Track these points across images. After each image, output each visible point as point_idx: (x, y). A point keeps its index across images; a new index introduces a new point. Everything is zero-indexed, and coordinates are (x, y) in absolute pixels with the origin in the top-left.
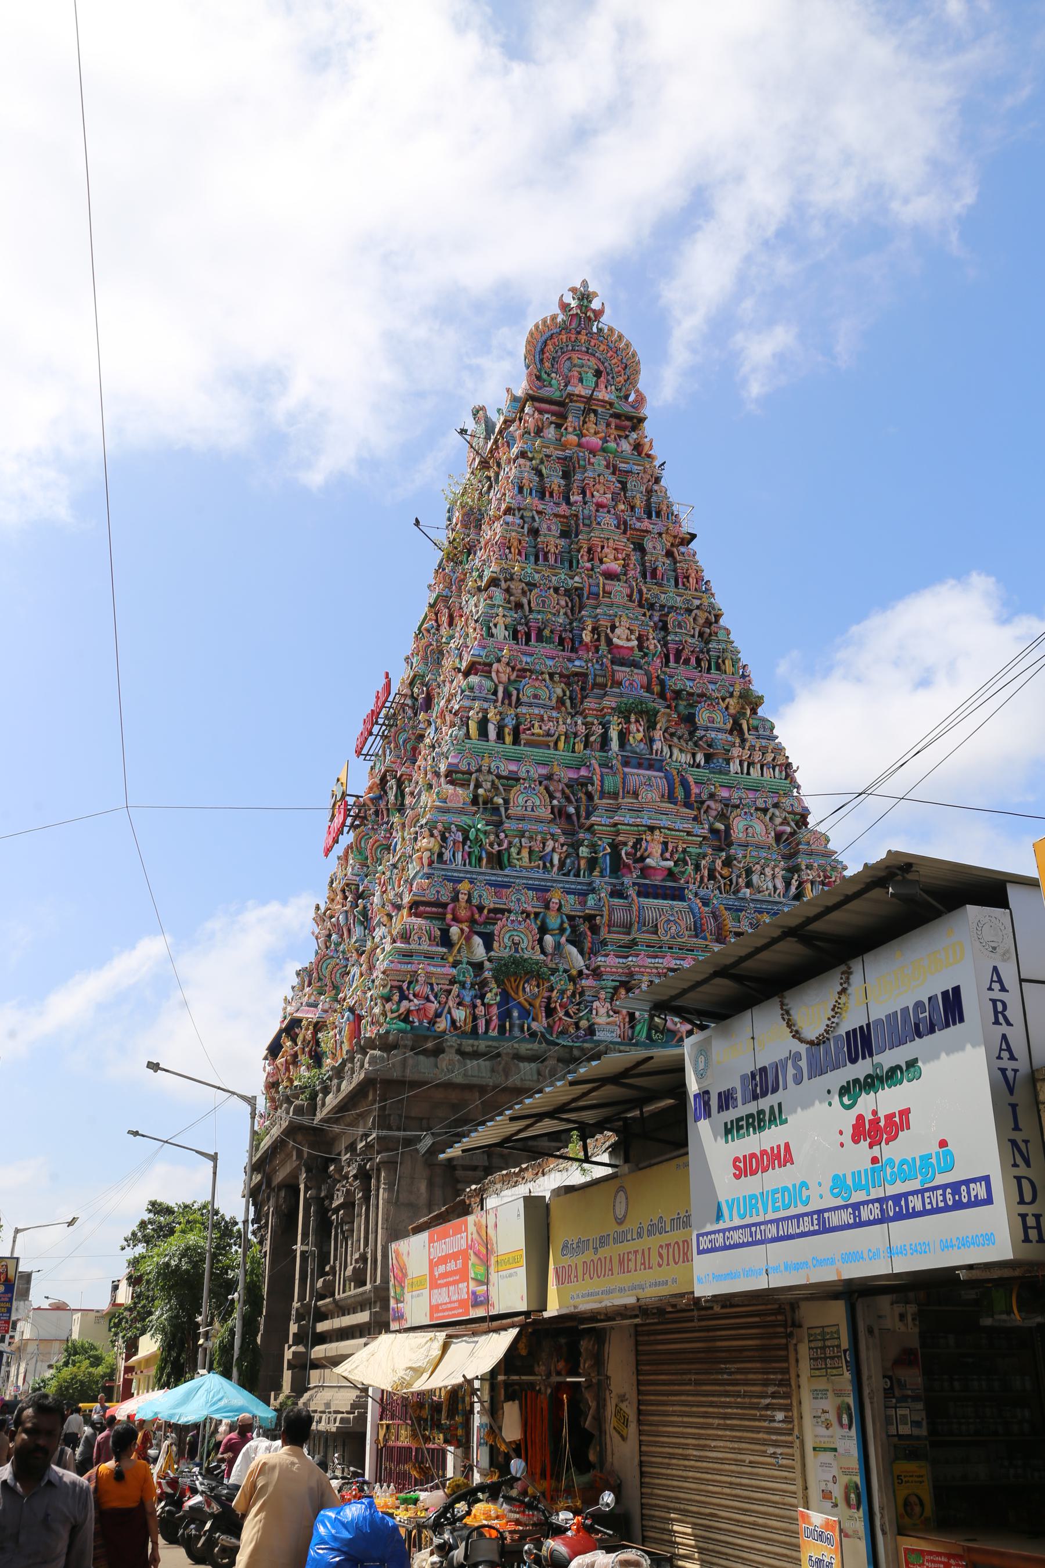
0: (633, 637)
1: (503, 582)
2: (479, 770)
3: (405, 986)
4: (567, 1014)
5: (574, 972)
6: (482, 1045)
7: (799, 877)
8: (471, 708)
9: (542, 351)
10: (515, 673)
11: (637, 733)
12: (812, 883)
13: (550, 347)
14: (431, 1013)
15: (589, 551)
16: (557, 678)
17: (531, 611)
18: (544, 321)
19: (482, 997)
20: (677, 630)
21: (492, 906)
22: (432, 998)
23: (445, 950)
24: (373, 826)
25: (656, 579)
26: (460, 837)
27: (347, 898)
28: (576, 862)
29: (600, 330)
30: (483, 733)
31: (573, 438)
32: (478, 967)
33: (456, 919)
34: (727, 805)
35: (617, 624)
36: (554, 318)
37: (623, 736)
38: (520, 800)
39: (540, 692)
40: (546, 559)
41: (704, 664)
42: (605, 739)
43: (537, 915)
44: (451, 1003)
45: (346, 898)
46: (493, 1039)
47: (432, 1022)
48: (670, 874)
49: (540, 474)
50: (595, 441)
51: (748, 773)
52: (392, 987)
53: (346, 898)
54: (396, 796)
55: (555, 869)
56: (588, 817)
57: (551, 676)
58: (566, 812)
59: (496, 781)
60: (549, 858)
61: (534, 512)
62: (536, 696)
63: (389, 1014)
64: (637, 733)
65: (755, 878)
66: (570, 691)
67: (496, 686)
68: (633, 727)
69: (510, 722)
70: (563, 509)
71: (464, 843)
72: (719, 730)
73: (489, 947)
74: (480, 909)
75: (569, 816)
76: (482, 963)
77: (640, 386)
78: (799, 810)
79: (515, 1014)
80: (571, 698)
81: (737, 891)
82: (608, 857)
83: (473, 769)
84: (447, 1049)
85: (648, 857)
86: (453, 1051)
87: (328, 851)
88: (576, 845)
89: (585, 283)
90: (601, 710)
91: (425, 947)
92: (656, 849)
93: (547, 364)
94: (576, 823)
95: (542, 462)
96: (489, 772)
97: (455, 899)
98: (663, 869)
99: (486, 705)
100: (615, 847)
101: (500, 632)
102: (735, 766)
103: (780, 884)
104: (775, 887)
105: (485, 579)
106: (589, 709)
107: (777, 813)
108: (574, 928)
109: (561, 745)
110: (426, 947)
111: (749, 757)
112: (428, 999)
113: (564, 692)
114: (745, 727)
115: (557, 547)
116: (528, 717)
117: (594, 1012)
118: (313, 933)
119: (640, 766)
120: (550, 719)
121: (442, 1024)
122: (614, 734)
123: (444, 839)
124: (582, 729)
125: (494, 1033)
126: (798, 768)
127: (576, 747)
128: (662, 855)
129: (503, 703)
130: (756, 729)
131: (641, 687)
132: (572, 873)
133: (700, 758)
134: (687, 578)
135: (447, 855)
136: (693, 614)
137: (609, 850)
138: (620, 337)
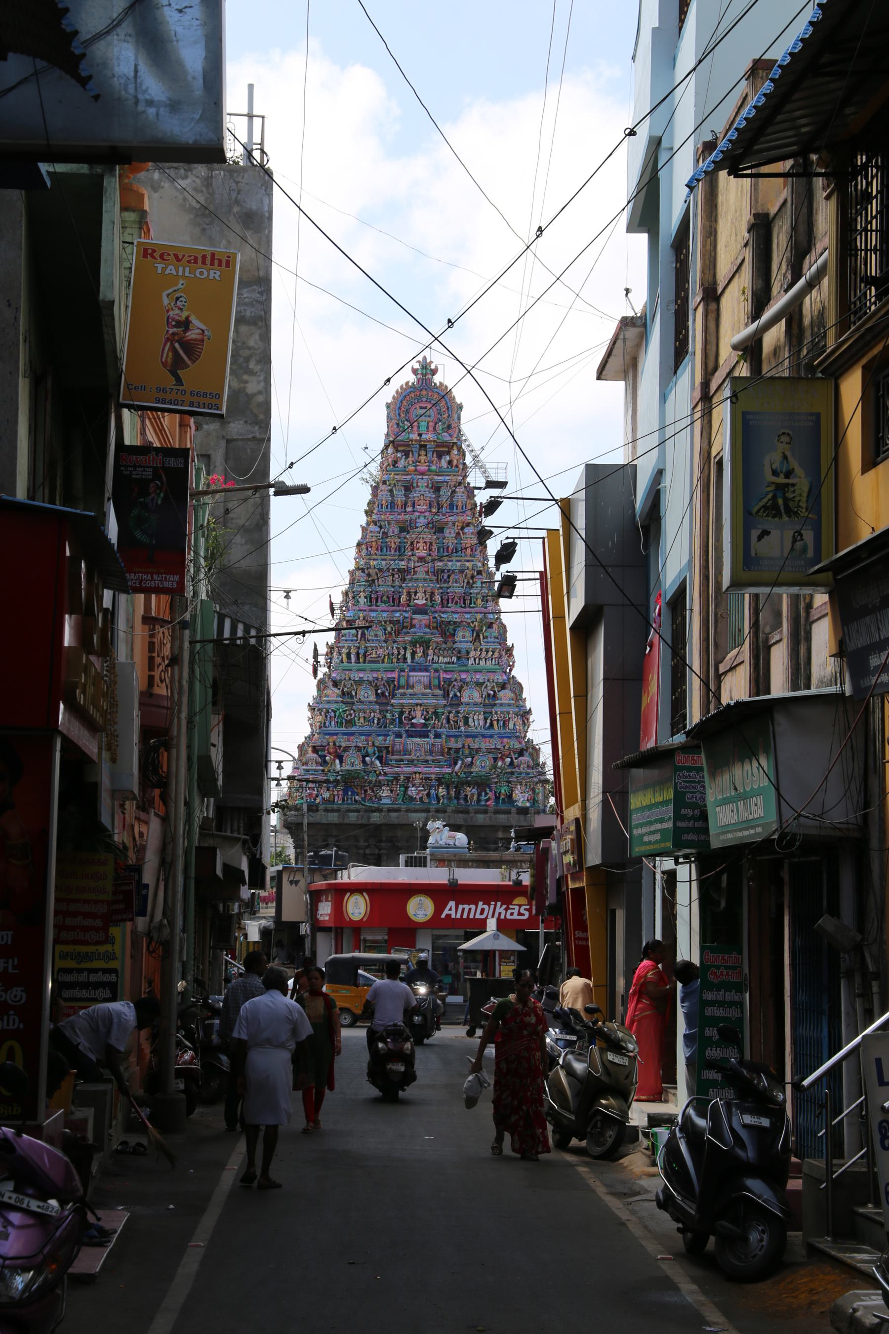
2: (345, 679)
4: (373, 791)
5: (378, 772)
6: (335, 807)
9: (400, 408)
11: (420, 651)
12: (498, 721)
13: (405, 403)
14: (314, 796)
15: (412, 543)
16: (388, 623)
20: (455, 585)
26: (333, 714)
37: (413, 654)
38: (362, 693)
39: (378, 633)
41: (468, 602)
42: (405, 659)
43: (365, 747)
46: (340, 804)
47: (315, 799)
48: (425, 725)
49: (392, 495)
50: (422, 468)
51: (479, 664)
55: (375, 725)
57: (385, 622)
62: (376, 635)
64: (420, 651)
68: (418, 650)
69: (362, 652)
74: (340, 746)
75: (386, 696)
76: (338, 772)
79: (350, 793)
80: (395, 632)
81: (459, 728)
83: (343, 678)
92: (419, 714)
93: (402, 415)
96: (350, 679)
97: (329, 744)
98: (422, 724)
100: (401, 713)
101: (362, 600)
102: (471, 661)
103: (482, 723)
109: (386, 660)
115: (395, 543)
119: (420, 670)
122: (408, 656)
123: (326, 717)
124: (395, 652)
125: (340, 802)
129: (361, 640)
131: (426, 626)
133: (454, 659)
135: (327, 724)
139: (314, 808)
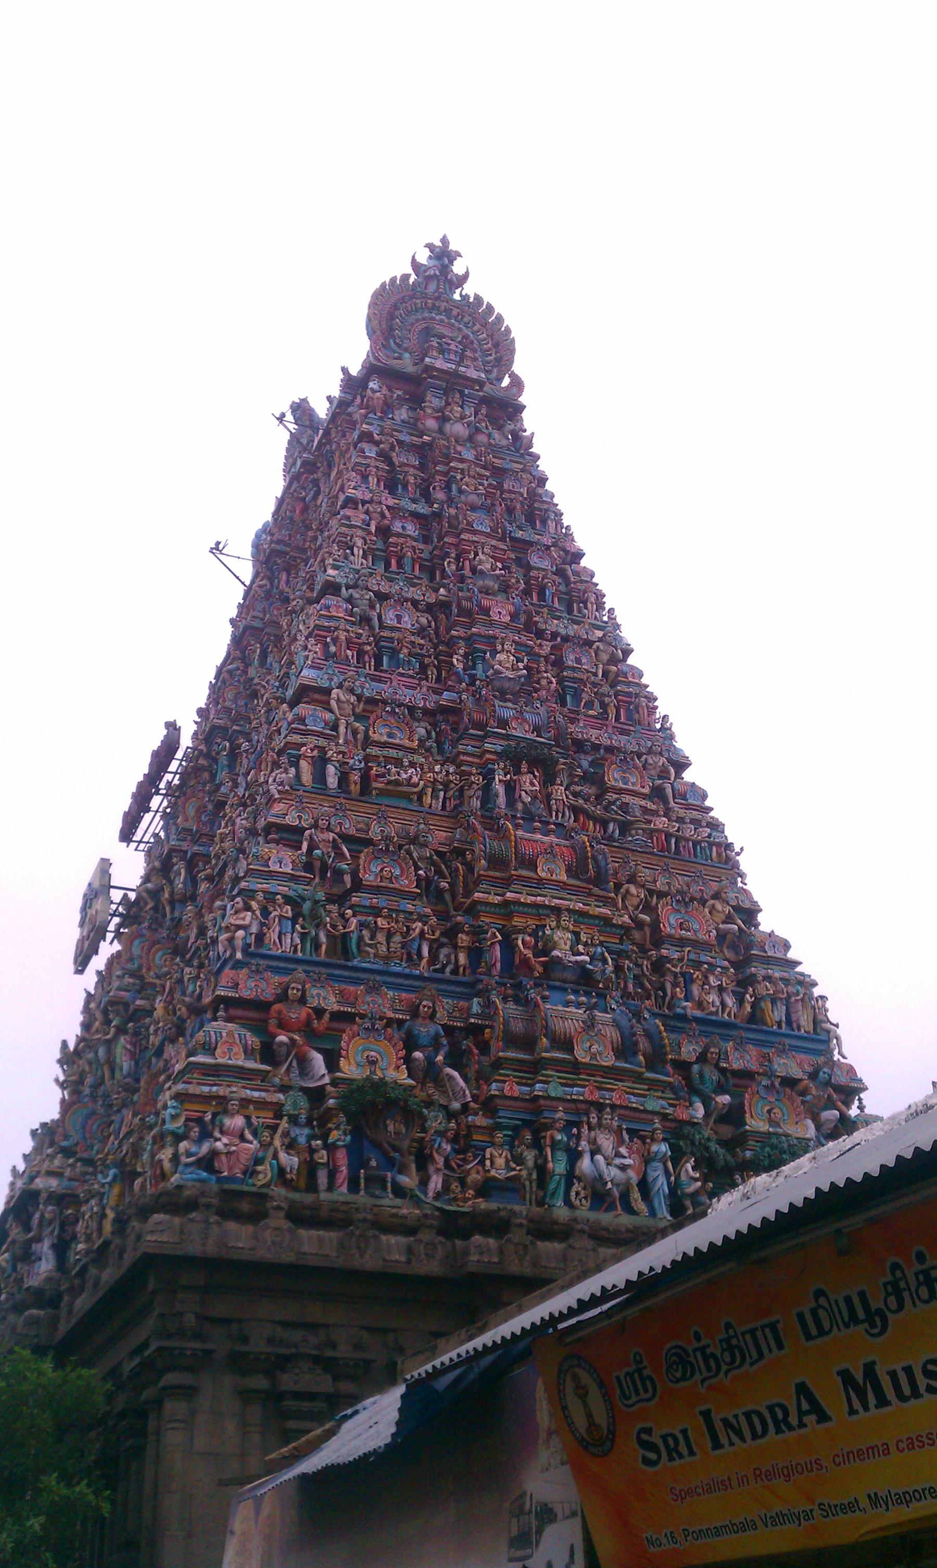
0: (521, 665)
1: (344, 589)
3: (208, 1117)
5: (456, 1105)
7: (754, 991)
8: (304, 745)
10: (361, 706)
17: (382, 626)
18: (393, 280)
19: (324, 1137)
21: (336, 1007)
22: (249, 1136)
23: (268, 1068)
24: (151, 924)
25: (545, 601)
27: (111, 1022)
28: (453, 957)
29: (465, 297)
30: (320, 777)
31: (431, 424)
32: (316, 1095)
33: (284, 1025)
34: (651, 892)
35: (499, 648)
36: (406, 277)
37: (510, 788)
40: (400, 565)
43: (400, 1023)
44: (277, 1142)
45: (110, 1022)
52: (188, 1120)
53: (108, 1022)
54: (184, 883)
56: (468, 893)
58: (437, 887)
59: (339, 841)
60: (415, 946)
61: (385, 507)
63: (184, 1160)
65: (695, 990)
66: (436, 733)
67: (337, 719)
70: (422, 508)
71: (294, 921)
72: (635, 794)
73: (332, 1062)
75: (440, 892)
76: (323, 1087)
77: (517, 368)
78: (747, 905)
82: (498, 947)
84: (272, 1212)
85: (554, 948)
86: (281, 1214)
87: (80, 971)
88: (451, 933)
89: (444, 240)
90: (480, 757)
91: (240, 1061)
94: (450, 904)
95: (392, 448)
99: (322, 742)
104: (723, 1004)
105: (318, 587)
106: (464, 754)
107: (719, 906)
108: (454, 1045)
110: (240, 1063)
111: (678, 831)
112: (242, 1138)
113: (429, 733)
114: (669, 791)
116: (381, 759)
117: (488, 1163)
118: (57, 1080)
120: (412, 765)
121: (266, 1172)
123: (265, 912)
126: (742, 849)
127: (448, 804)
128: (571, 949)
130: (684, 797)
132: (448, 970)
134: (585, 603)
136: (594, 647)
137: (500, 938)
138: (490, 308)
139: (245, 1206)
